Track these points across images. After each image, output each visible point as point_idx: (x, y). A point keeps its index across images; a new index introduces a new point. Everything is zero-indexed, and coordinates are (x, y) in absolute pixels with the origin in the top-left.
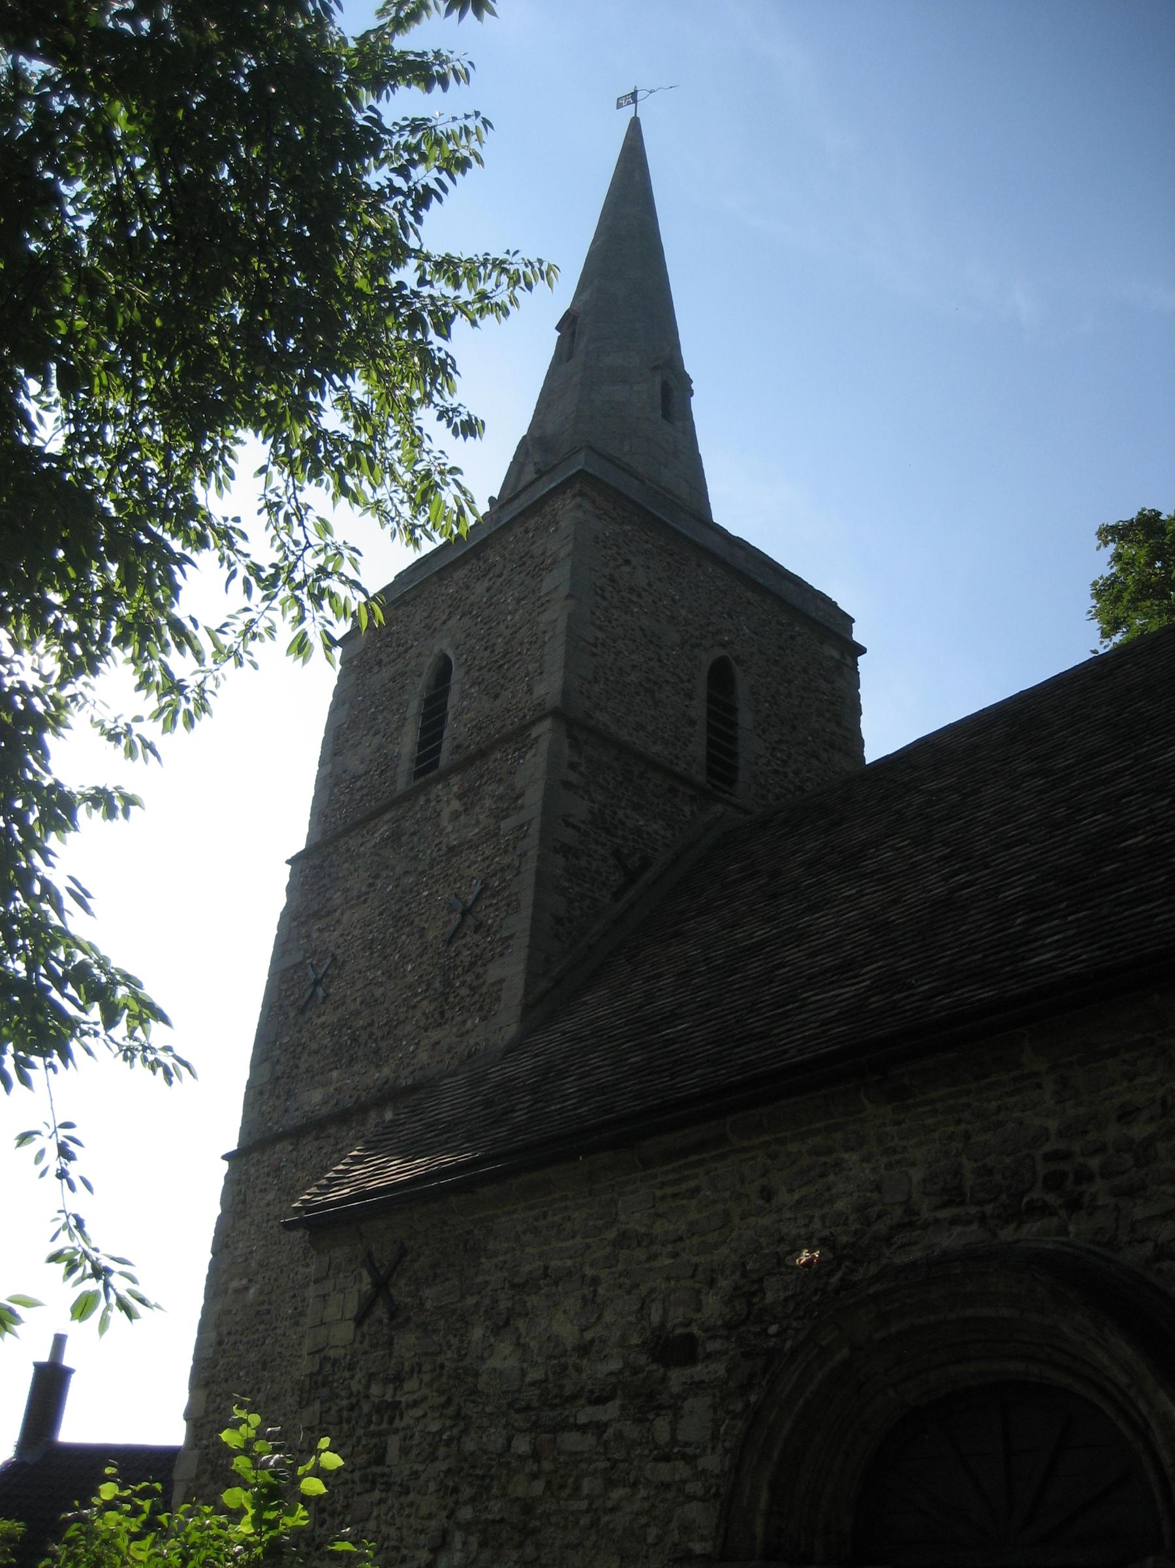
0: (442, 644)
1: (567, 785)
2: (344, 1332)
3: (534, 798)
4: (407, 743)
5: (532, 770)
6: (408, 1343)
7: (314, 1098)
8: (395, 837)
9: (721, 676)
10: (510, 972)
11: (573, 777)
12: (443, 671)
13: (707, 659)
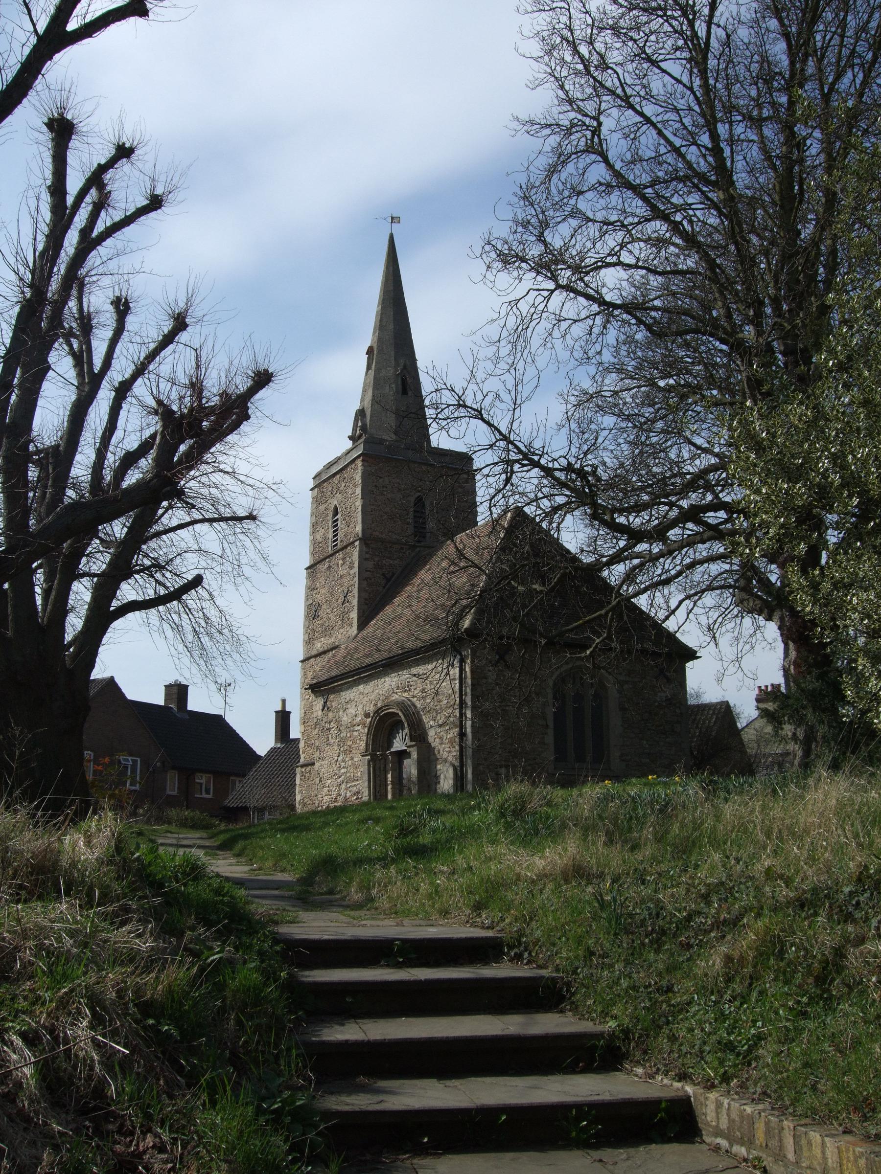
0: (335, 502)
1: (366, 559)
2: (320, 713)
3: (356, 565)
4: (330, 535)
5: (355, 555)
6: (331, 714)
7: (318, 646)
8: (330, 567)
9: (419, 501)
10: (354, 615)
11: (368, 556)
12: (336, 512)
13: (412, 499)
